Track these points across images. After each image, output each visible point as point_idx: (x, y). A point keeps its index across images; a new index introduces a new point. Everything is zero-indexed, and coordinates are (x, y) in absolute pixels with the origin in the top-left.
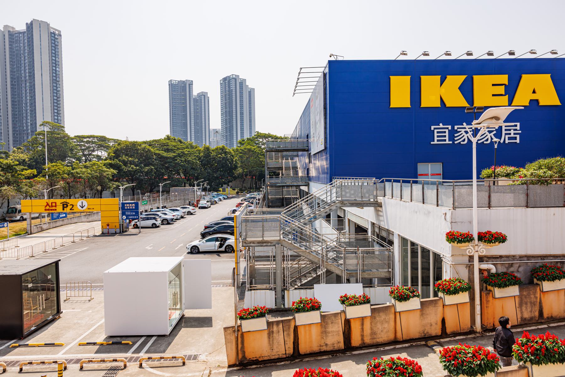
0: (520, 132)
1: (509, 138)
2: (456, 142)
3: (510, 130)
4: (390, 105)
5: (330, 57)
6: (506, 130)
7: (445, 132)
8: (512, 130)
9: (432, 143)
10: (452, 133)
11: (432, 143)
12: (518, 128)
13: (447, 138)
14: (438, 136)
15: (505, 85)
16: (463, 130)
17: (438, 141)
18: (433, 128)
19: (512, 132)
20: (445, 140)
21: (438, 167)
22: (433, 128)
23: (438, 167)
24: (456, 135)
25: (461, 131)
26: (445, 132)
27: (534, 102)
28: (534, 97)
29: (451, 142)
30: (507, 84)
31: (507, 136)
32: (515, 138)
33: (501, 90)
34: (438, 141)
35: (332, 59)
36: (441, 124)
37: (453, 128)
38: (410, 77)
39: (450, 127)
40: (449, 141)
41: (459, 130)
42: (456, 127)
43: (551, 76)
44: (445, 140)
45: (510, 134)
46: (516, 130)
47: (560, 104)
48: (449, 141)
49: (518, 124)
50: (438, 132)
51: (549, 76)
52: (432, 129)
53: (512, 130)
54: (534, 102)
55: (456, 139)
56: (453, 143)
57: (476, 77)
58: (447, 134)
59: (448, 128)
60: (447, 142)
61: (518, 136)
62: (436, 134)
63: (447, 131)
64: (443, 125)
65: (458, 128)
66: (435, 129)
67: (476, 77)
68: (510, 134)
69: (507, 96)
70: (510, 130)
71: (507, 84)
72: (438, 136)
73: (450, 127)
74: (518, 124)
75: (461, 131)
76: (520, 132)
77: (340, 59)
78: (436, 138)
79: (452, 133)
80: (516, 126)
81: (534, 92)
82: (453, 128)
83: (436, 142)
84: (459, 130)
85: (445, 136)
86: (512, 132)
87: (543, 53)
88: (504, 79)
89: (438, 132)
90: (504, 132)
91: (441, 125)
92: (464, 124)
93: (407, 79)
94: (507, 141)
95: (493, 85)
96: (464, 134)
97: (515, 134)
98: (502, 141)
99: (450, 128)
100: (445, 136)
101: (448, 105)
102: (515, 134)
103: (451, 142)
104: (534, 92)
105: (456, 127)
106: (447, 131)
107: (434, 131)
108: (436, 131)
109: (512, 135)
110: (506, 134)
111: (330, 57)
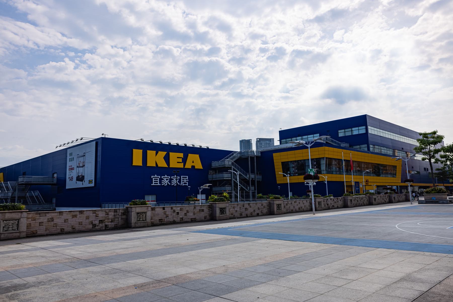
0: (188, 180)
1: (184, 183)
2: (162, 185)
3: (184, 179)
4: (132, 164)
5: (102, 135)
6: (183, 179)
7: (157, 179)
8: (185, 179)
9: (152, 185)
10: (161, 180)
11: (152, 185)
12: (187, 178)
13: (158, 182)
14: (155, 181)
15: (182, 158)
16: (165, 179)
17: (155, 183)
18: (152, 177)
19: (185, 180)
20: (157, 183)
21: (154, 197)
22: (152, 177)
23: (154, 197)
24: (162, 181)
25: (164, 179)
26: (157, 179)
27: (193, 167)
28: (193, 164)
29: (160, 185)
30: (183, 157)
31: (183, 182)
32: (186, 183)
33: (180, 160)
34: (155, 183)
35: (103, 136)
36: (156, 175)
37: (161, 177)
38: (142, 150)
39: (160, 177)
40: (159, 184)
41: (163, 178)
42: (162, 177)
43: (199, 156)
44: (157, 183)
45: (184, 181)
46: (186, 179)
47: (202, 168)
48: (159, 184)
49: (187, 177)
50: (154, 179)
51: (198, 155)
52: (152, 177)
53: (185, 179)
54: (193, 167)
55: (162, 183)
56: (161, 185)
57: (171, 153)
58: (158, 180)
59: (158, 177)
60: (159, 184)
61: (187, 182)
62: (154, 180)
63: (158, 178)
64: (157, 176)
65: (163, 178)
66: (153, 177)
67: (171, 153)
68: (184, 181)
69: (183, 163)
70: (184, 179)
71: (183, 157)
72: (155, 181)
73: (160, 177)
74: (187, 177)
75: (164, 179)
76: (188, 180)
77: (107, 137)
78: (154, 182)
79: (161, 180)
80: (186, 177)
81: (193, 162)
82: (161, 177)
83: (153, 184)
84: (163, 178)
85: (157, 181)
86: (185, 180)
87: (197, 145)
88: (181, 155)
89: (154, 179)
90: (182, 180)
91: (156, 176)
92: (166, 175)
93: (141, 151)
94: (183, 185)
95: (178, 158)
96: (166, 180)
97: (186, 181)
98: (181, 185)
99: (160, 178)
100: (157, 181)
101: (159, 166)
102: (186, 181)
103: (160, 185)
104: (193, 162)
105: (162, 177)
106: (158, 178)
107: (152, 178)
108: (153, 178)
109: (185, 182)
110: (183, 181)
111: (102, 135)
